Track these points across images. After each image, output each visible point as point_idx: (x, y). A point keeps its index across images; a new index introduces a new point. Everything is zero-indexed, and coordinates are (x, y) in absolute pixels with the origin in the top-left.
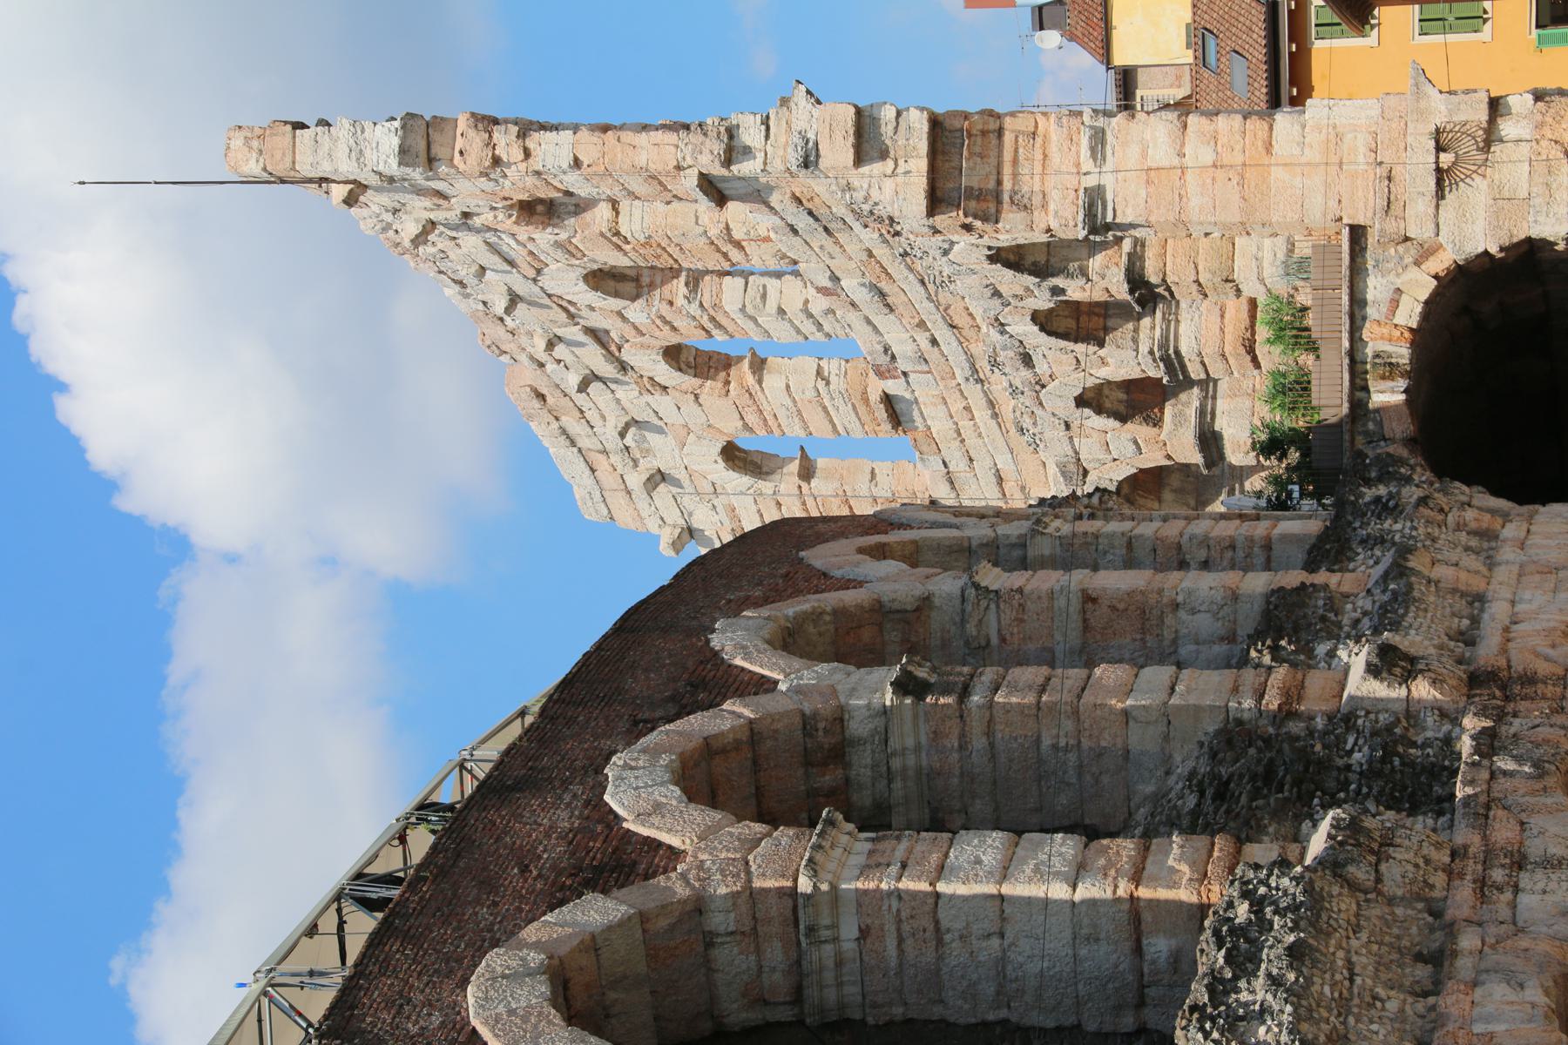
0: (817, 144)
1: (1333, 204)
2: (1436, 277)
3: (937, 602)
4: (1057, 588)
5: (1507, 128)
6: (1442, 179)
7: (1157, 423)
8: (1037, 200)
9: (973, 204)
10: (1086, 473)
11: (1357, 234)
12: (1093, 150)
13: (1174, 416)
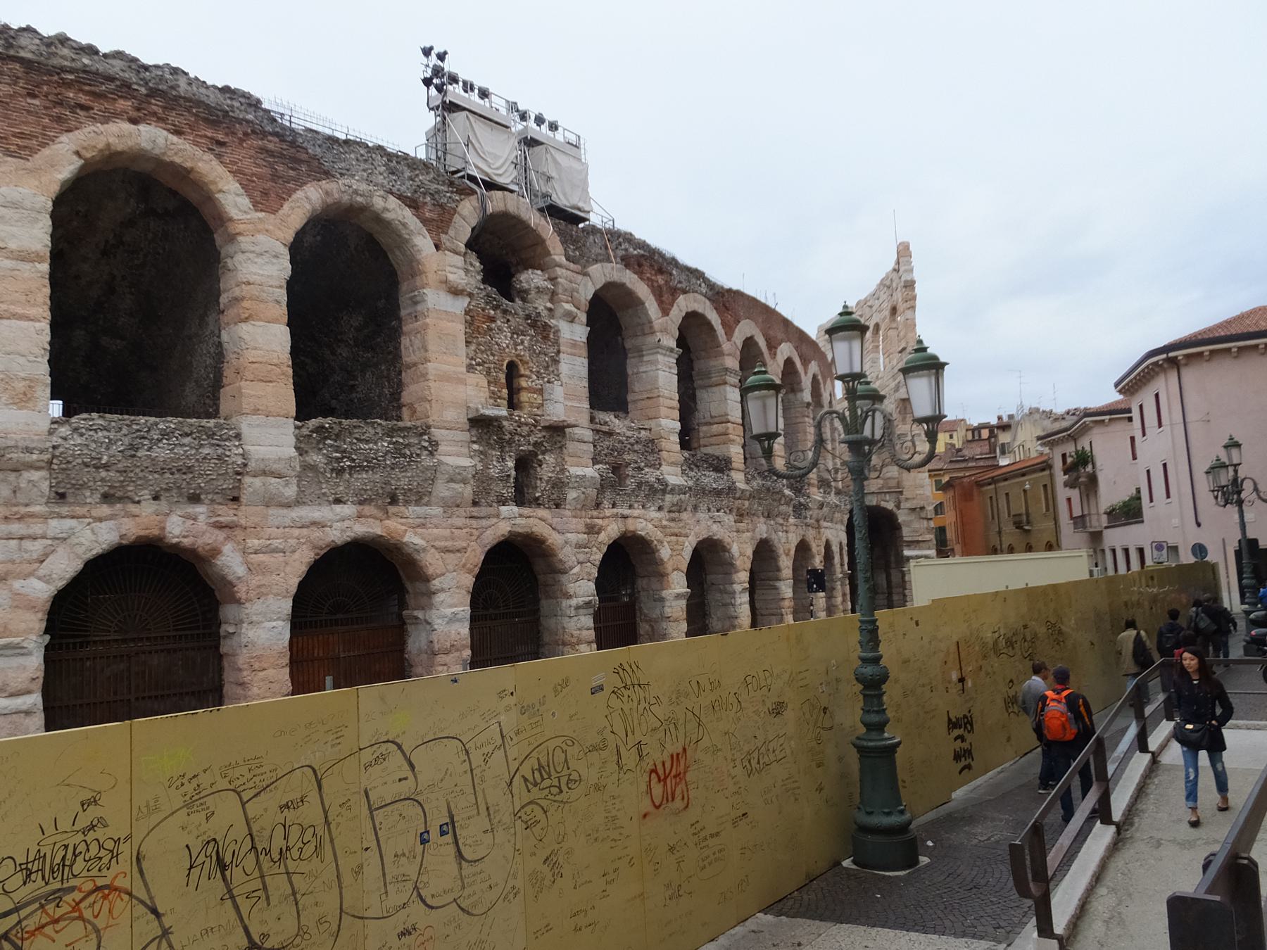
6: (913, 510)
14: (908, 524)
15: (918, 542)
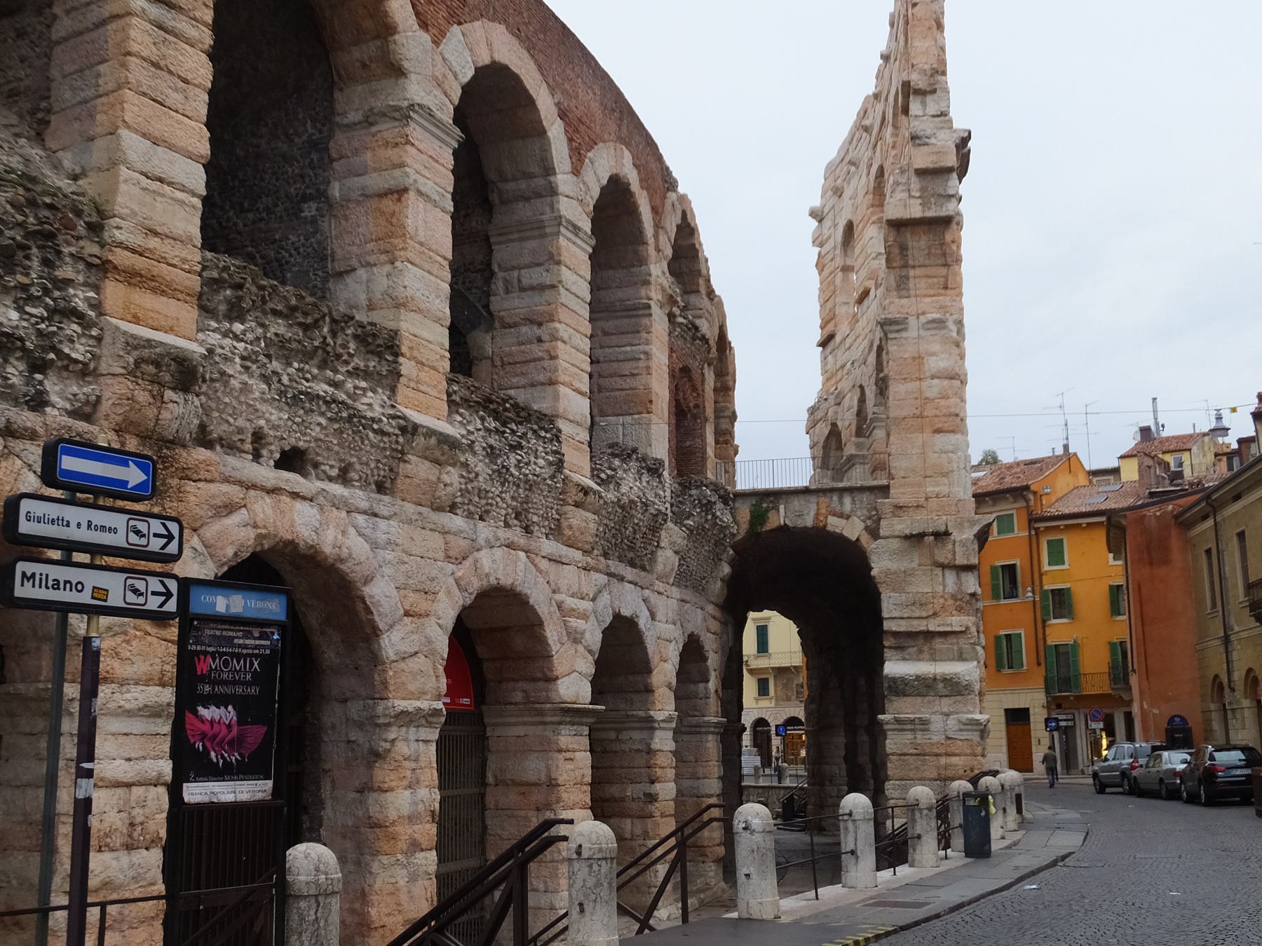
0: (927, 144)
1: (902, 473)
2: (858, 539)
3: (402, 80)
4: (407, 169)
5: (950, 577)
6: (915, 539)
8: (904, 293)
9: (896, 251)
11: (884, 490)
12: (933, 321)
14: (901, 580)
15: (929, 635)
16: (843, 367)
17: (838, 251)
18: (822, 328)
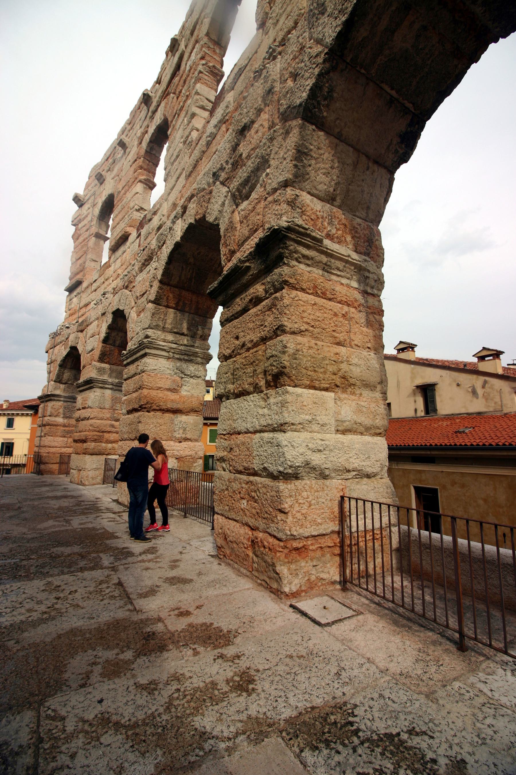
7: (101, 359)
10: (82, 331)
13: (104, 368)
16: (86, 305)
17: (94, 222)
18: (71, 279)
